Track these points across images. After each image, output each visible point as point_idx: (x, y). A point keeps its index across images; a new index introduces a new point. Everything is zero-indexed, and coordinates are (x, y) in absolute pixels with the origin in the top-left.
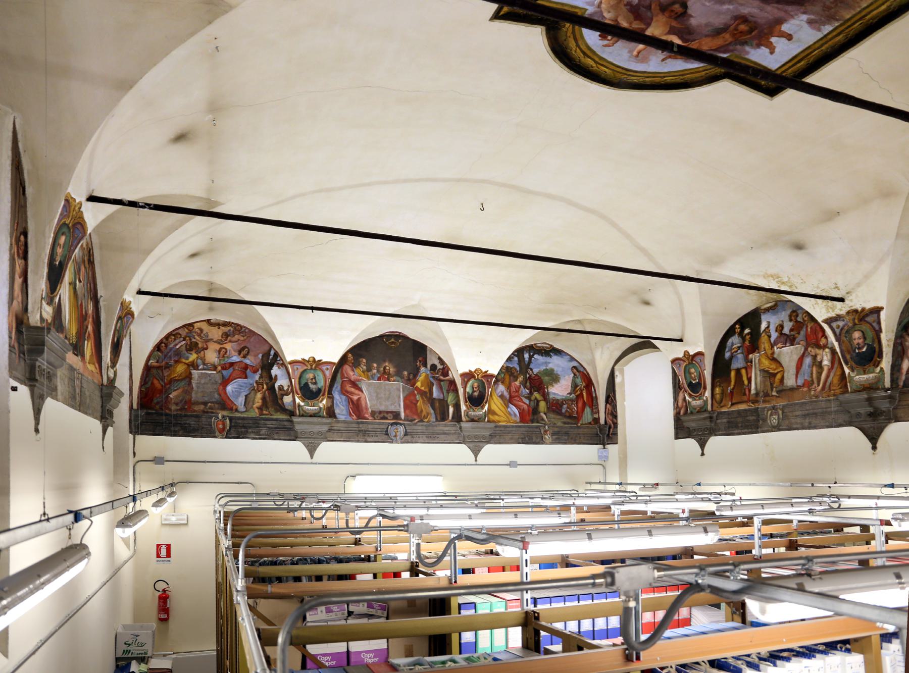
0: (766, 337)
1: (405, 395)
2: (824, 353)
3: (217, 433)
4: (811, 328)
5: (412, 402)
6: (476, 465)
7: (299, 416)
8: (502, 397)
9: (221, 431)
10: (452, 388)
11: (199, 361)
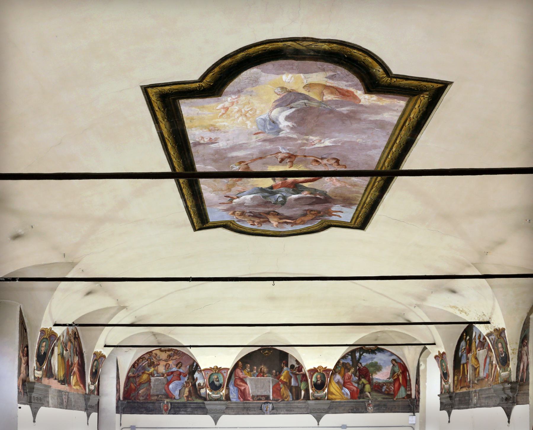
0: (474, 342)
1: (274, 384)
3: (164, 412)
5: (277, 389)
6: (318, 427)
7: (209, 400)
8: (338, 383)
9: (166, 410)
10: (304, 379)
11: (155, 372)
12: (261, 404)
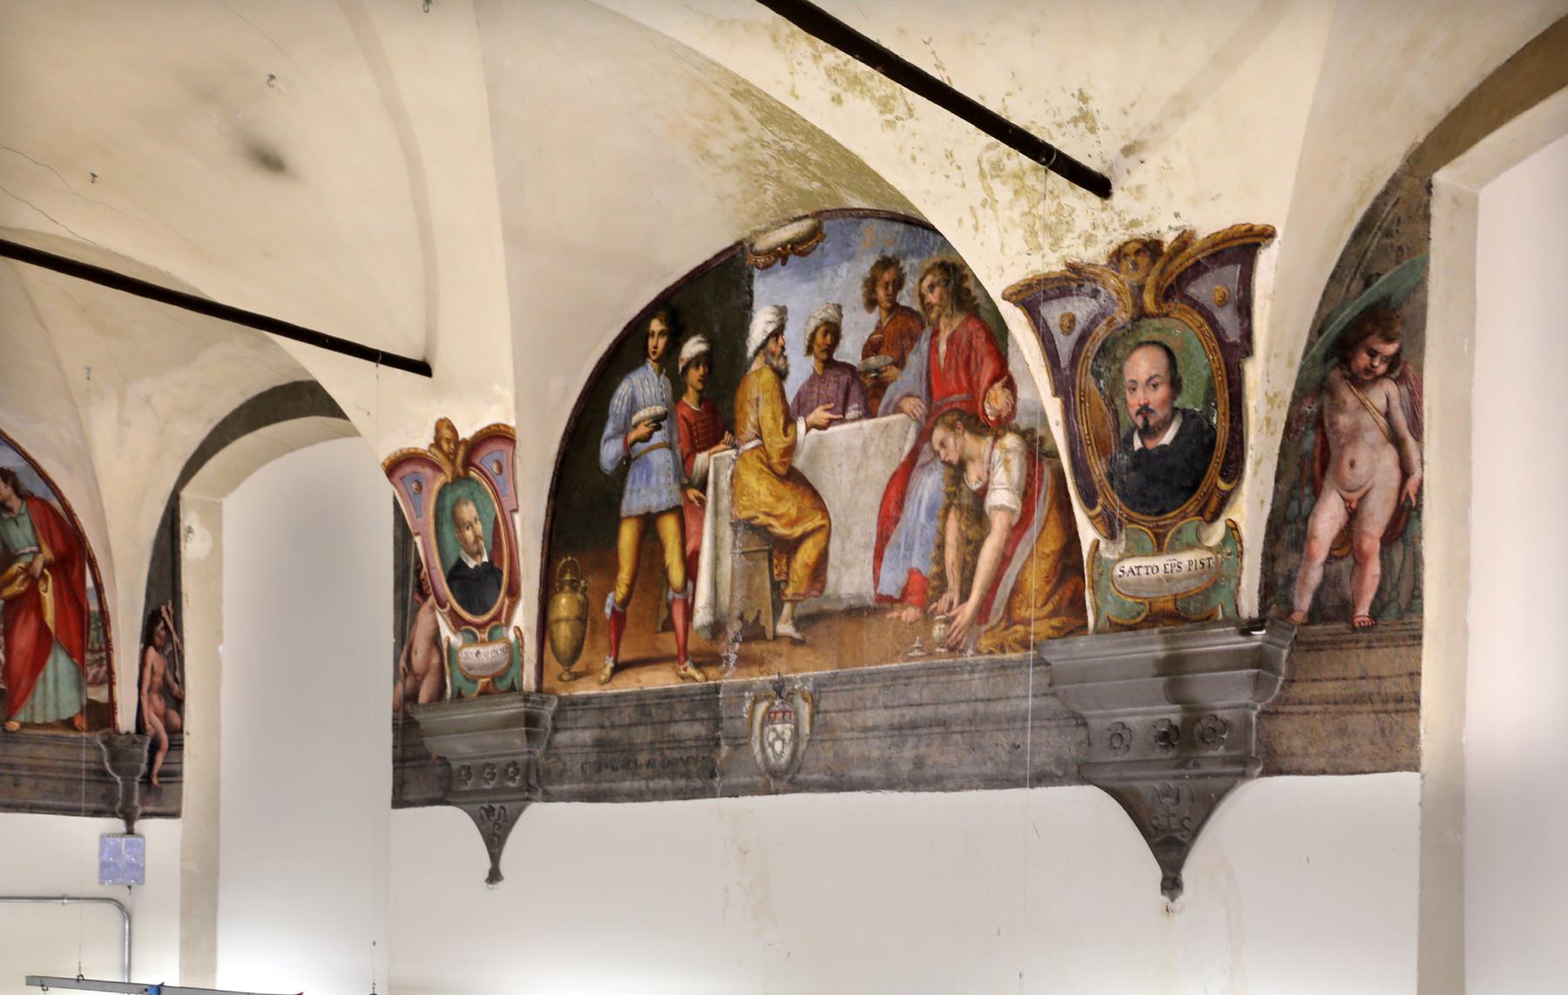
0: (768, 375)
2: (997, 453)
4: (950, 341)
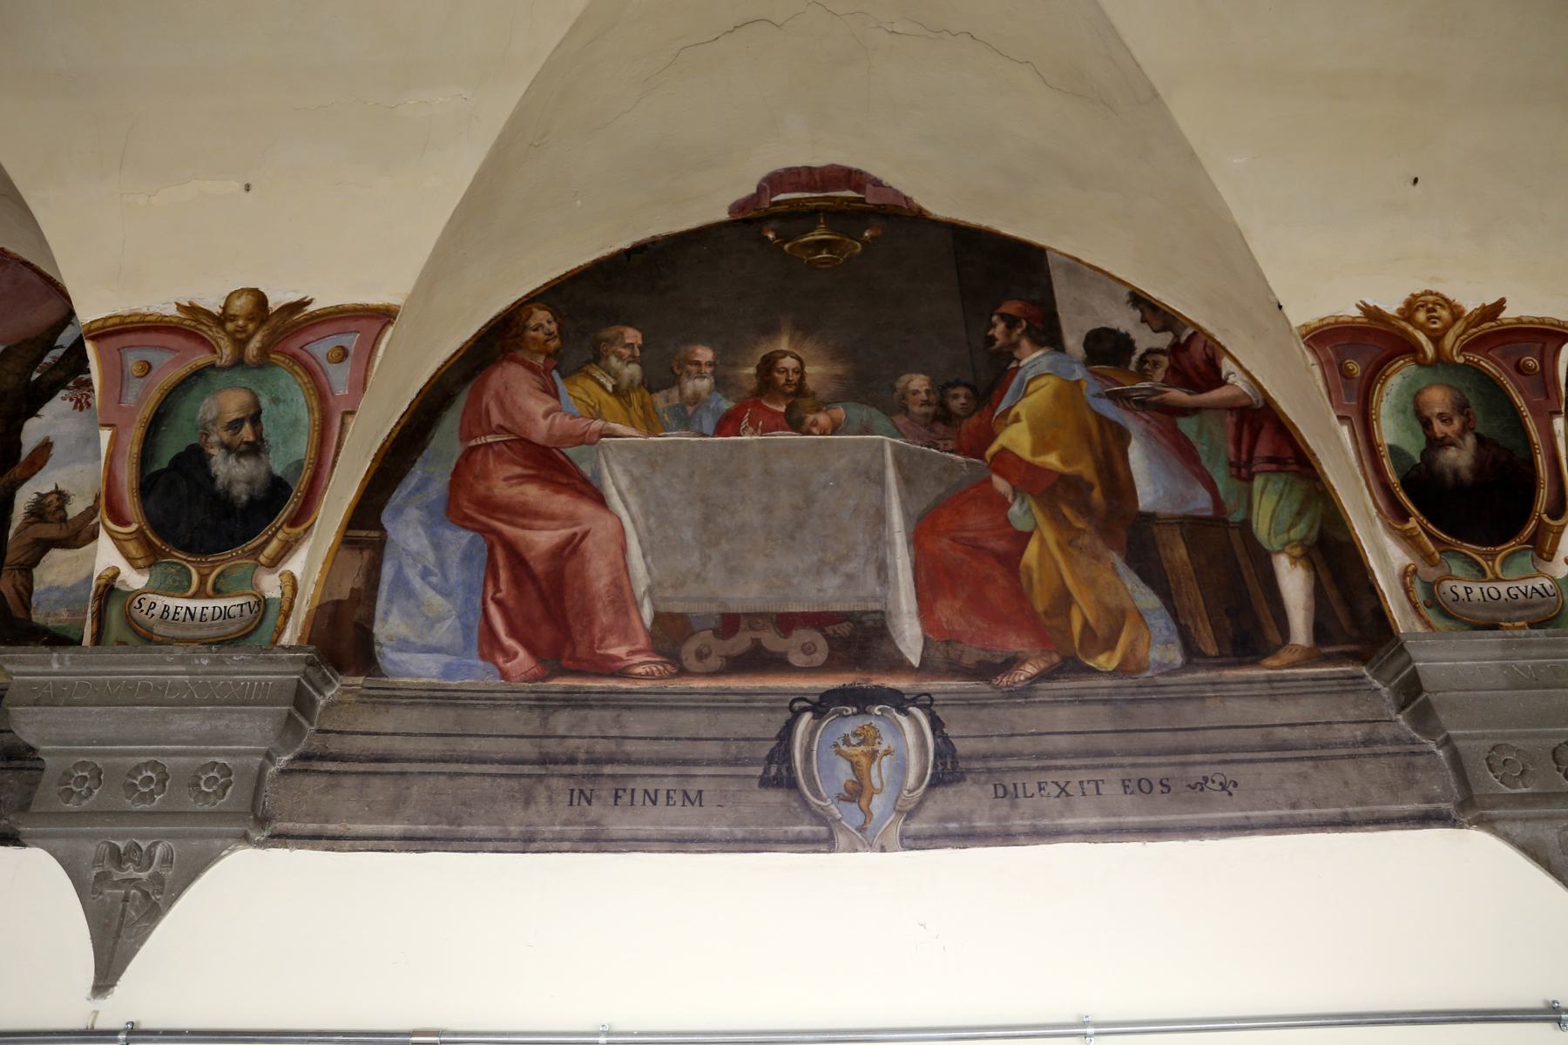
1: (920, 505)
10: (1263, 448)
12: (783, 717)
